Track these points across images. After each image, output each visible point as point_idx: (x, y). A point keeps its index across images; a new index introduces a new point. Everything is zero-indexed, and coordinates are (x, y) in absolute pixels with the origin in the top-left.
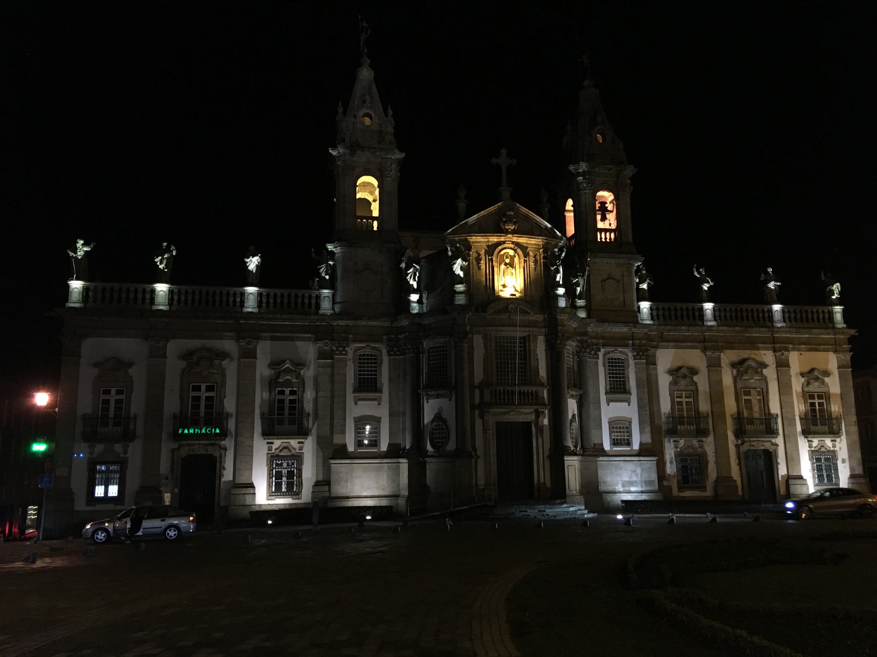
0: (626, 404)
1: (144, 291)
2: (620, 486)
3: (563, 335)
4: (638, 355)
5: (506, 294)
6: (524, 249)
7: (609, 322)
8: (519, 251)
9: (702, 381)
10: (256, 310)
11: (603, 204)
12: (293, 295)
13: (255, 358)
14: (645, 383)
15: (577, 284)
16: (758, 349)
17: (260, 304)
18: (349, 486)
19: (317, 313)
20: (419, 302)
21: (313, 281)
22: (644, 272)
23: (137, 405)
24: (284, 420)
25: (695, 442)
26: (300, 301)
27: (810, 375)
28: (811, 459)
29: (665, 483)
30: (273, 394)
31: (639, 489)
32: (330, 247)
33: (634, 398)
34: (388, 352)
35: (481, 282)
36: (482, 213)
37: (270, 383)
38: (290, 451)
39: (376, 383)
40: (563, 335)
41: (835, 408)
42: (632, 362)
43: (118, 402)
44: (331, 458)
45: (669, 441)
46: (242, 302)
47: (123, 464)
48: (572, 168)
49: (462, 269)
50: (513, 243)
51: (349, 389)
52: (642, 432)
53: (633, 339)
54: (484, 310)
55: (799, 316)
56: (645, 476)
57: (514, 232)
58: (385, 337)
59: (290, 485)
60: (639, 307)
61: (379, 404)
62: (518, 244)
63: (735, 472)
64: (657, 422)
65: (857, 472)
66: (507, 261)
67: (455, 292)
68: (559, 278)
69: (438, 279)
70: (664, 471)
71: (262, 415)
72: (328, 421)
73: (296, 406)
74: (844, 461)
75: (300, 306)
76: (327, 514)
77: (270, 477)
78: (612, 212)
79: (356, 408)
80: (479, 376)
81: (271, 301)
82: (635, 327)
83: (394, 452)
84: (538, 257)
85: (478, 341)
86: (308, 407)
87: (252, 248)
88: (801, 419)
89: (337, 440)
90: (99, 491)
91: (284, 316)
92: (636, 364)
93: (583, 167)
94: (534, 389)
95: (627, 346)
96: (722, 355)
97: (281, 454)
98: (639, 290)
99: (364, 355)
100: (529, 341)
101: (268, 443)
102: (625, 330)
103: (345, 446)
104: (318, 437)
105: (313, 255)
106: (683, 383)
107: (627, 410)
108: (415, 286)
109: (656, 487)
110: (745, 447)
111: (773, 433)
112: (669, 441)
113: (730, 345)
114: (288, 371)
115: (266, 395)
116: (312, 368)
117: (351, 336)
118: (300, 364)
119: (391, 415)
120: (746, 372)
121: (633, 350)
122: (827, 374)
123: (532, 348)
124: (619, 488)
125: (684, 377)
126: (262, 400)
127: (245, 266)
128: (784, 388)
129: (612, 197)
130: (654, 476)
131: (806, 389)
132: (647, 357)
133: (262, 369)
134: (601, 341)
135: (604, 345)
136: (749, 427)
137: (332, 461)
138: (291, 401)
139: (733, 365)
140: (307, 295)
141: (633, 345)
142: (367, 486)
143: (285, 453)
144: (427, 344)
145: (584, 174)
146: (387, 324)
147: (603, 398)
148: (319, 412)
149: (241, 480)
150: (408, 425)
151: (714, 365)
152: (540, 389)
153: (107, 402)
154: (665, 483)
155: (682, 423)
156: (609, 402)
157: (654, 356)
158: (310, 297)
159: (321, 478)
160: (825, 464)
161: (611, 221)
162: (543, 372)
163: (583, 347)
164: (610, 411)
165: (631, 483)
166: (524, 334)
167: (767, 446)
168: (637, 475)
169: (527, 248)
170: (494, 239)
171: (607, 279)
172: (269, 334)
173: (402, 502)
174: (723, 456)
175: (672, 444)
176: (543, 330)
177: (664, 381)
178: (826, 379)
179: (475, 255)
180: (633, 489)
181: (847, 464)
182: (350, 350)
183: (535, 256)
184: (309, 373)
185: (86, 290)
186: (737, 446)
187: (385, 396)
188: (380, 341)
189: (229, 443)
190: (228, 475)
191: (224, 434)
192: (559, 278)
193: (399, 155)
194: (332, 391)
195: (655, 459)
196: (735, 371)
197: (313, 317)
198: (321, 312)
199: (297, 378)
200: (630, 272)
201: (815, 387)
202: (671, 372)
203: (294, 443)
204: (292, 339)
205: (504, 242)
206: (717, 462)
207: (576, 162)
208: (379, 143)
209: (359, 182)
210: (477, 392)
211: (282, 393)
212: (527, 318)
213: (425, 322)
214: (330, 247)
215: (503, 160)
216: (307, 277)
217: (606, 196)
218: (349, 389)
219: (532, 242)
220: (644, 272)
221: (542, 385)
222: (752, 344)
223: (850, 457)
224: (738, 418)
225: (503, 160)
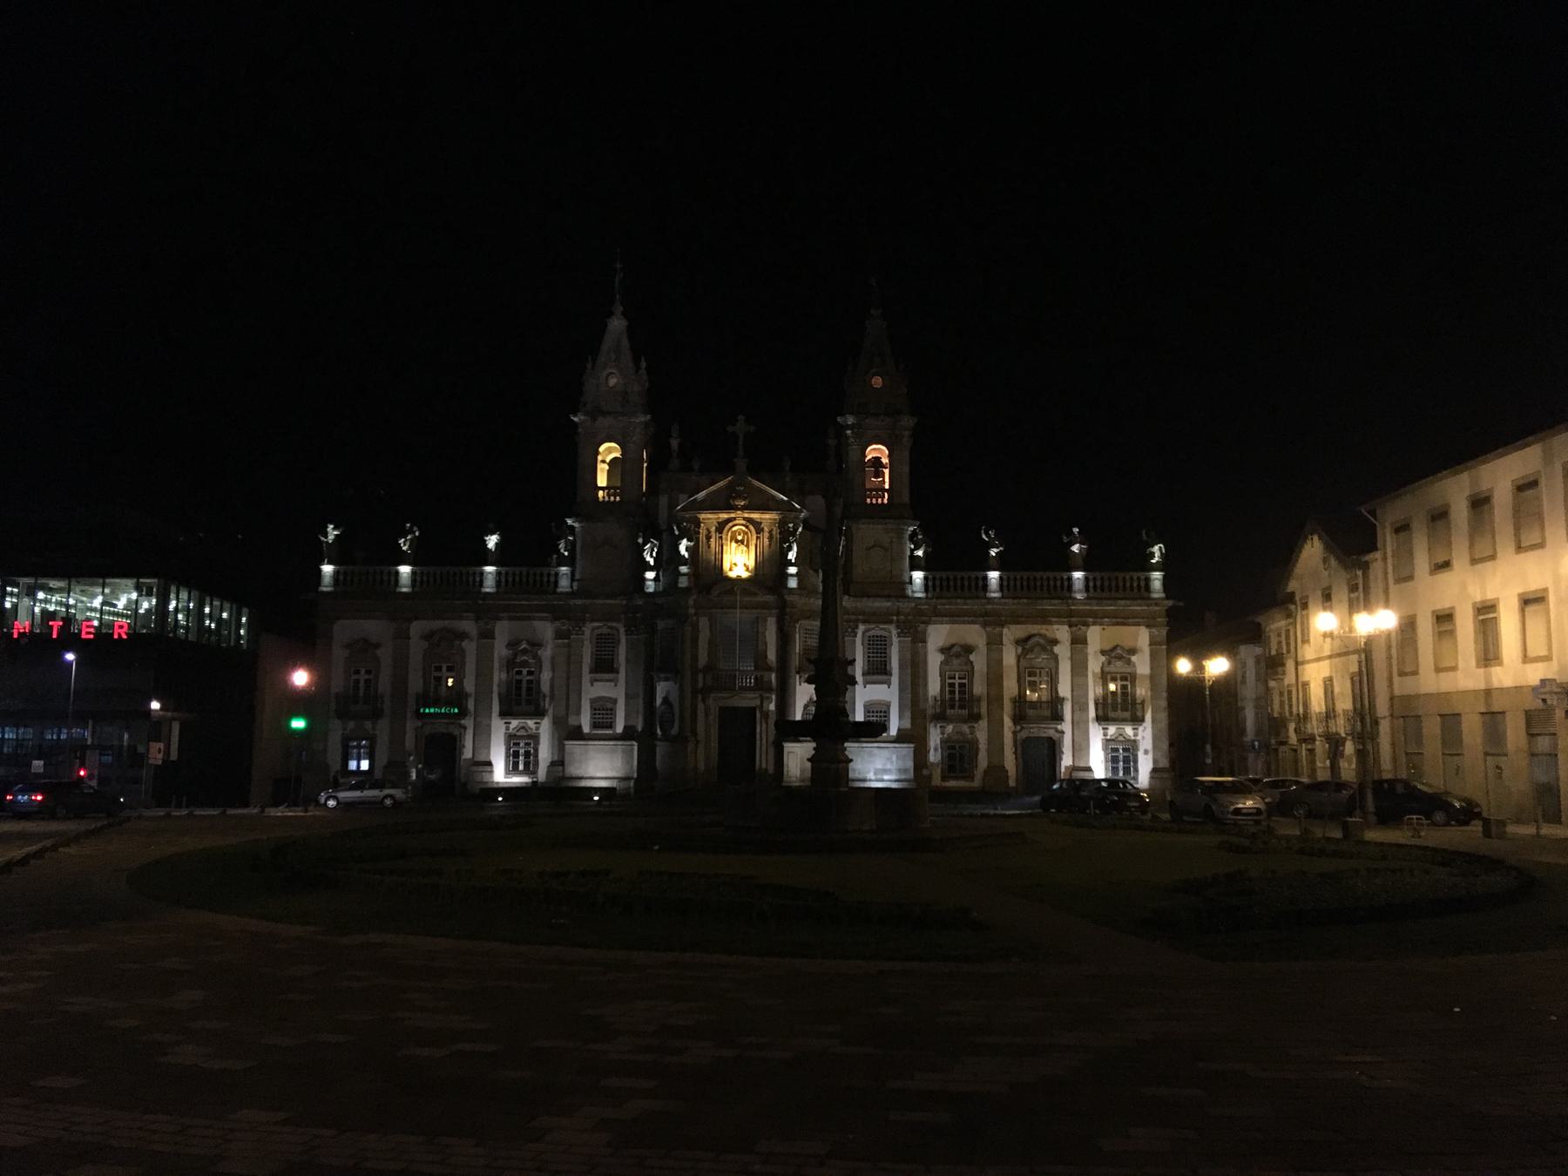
1: (389, 573)
5: (733, 575)
9: (979, 661)
11: (878, 459)
16: (1051, 623)
19: (555, 592)
20: (656, 579)
23: (384, 684)
24: (521, 700)
25: (965, 728)
27: (1117, 654)
28: (1105, 748)
29: (925, 772)
33: (895, 679)
41: (1142, 691)
42: (895, 640)
43: (366, 681)
46: (481, 582)
47: (372, 740)
48: (839, 419)
51: (586, 669)
52: (900, 717)
53: (898, 614)
55: (1106, 583)
57: (744, 508)
59: (527, 764)
62: (750, 520)
63: (1010, 761)
65: (1161, 765)
68: (792, 556)
69: (668, 560)
73: (533, 687)
74: (1146, 752)
76: (557, 794)
77: (507, 756)
79: (594, 689)
80: (703, 660)
83: (628, 734)
85: (704, 623)
88: (1096, 704)
89: (572, 721)
90: (353, 765)
95: (891, 622)
96: (1005, 631)
98: (912, 557)
103: (580, 727)
106: (956, 662)
107: (887, 693)
109: (911, 775)
110: (1024, 734)
111: (1059, 718)
113: (1016, 619)
114: (525, 651)
115: (504, 676)
118: (536, 644)
119: (627, 695)
120: (1031, 650)
122: (1133, 651)
124: (871, 776)
125: (958, 656)
127: (484, 543)
128: (1079, 668)
130: (910, 764)
131: (1107, 669)
133: (500, 650)
135: (864, 622)
136: (1031, 712)
138: (530, 682)
139: (1018, 642)
142: (601, 767)
143: (523, 733)
144: (661, 625)
145: (851, 427)
149: (482, 758)
150: (641, 709)
151: (995, 643)
153: (357, 681)
154: (925, 772)
155: (952, 707)
156: (866, 683)
157: (924, 632)
160: (1122, 755)
162: (772, 655)
165: (885, 771)
167: (1051, 733)
173: (632, 784)
174: (998, 742)
177: (934, 661)
178: (1134, 658)
181: (1150, 756)
182: (587, 629)
184: (546, 653)
185: (336, 574)
186: (1015, 733)
189: (468, 722)
190: (468, 753)
191: (463, 713)
192: (792, 556)
193: (643, 418)
196: (1020, 650)
201: (1119, 667)
202: (942, 650)
203: (531, 723)
204: (529, 618)
206: (988, 751)
207: (843, 415)
209: (602, 449)
211: (519, 673)
213: (659, 601)
214: (569, 522)
215: (740, 427)
216: (544, 553)
217: (877, 451)
218: (586, 669)
219: (767, 518)
221: (770, 669)
222: (1044, 618)
223: (1155, 747)
224: (1020, 701)
225: (740, 427)
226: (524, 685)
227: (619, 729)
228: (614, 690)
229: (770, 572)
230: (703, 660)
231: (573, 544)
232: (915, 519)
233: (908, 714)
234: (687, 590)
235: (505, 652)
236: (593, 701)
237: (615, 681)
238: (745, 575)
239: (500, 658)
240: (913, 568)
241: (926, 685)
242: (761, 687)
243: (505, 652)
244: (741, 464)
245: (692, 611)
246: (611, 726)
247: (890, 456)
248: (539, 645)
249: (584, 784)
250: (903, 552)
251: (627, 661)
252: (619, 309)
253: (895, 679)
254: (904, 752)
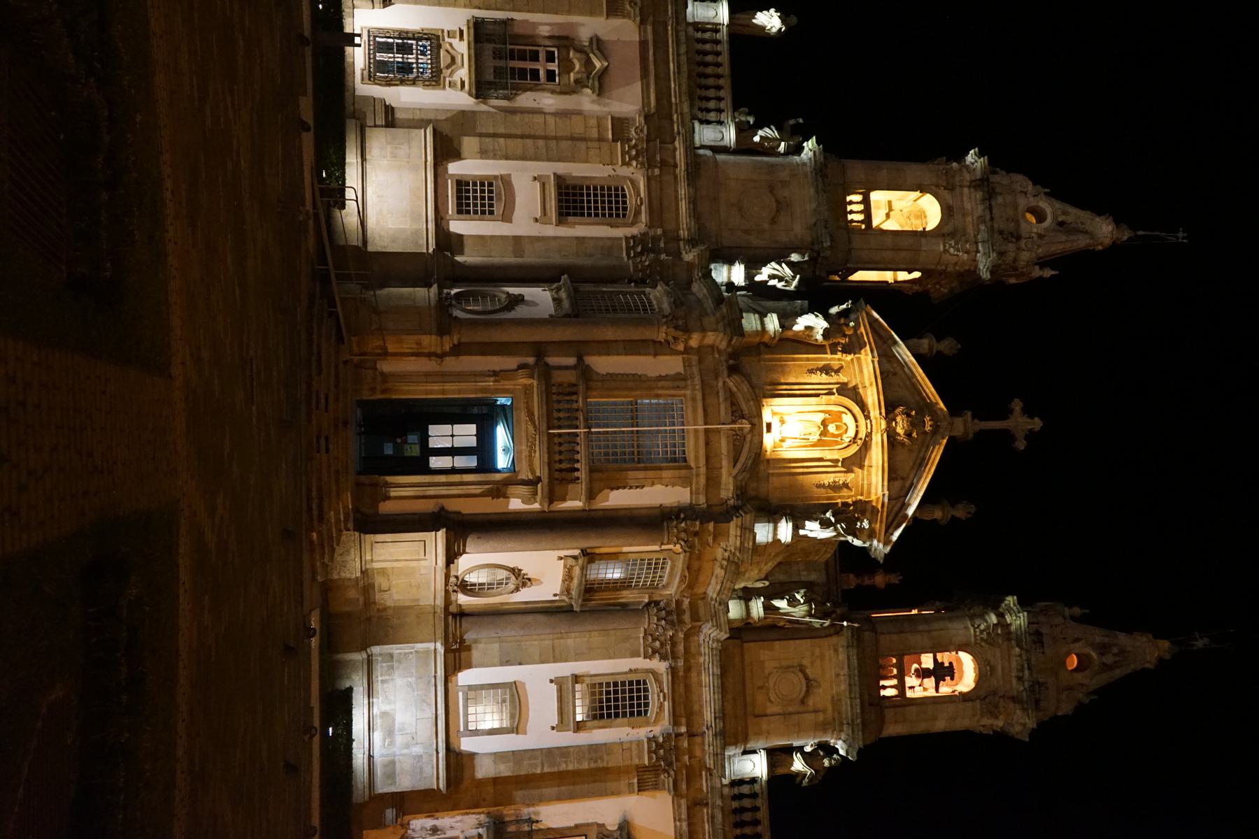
0: (555, 722)
2: (385, 708)
3: (696, 534)
4: (659, 746)
6: (856, 461)
7: (723, 674)
8: (854, 449)
10: (690, 19)
12: (721, 82)
13: (608, 16)
14: (600, 764)
15: (793, 602)
17: (699, 27)
18: (385, 162)
19: (694, 118)
20: (730, 286)
21: (749, 114)
22: (826, 763)
26: (712, 93)
29: (390, 813)
30: (547, 42)
31: (377, 752)
32: (810, 145)
34: (633, 237)
35: (783, 373)
36: (919, 372)
37: (567, 38)
38: (448, 67)
39: (575, 215)
40: (696, 534)
42: (642, 733)
44: (435, 130)
45: (480, 825)
48: (1011, 600)
49: (809, 328)
50: (869, 435)
51: (563, 168)
52: (499, 757)
53: (691, 735)
54: (733, 370)
56: (404, 765)
58: (659, 231)
60: (754, 752)
61: (536, 220)
62: (866, 446)
64: (519, 794)
66: (832, 428)
67: (763, 315)
68: (813, 529)
70: (418, 812)
71: (507, 23)
72: (502, 130)
75: (704, 93)
77: (403, 34)
78: (937, 689)
79: (528, 182)
80: (602, 364)
81: (708, 47)
82: (715, 735)
83: (448, 242)
84: (845, 492)
85: (671, 364)
86: (526, 100)
87: (794, 20)
91: (684, 58)
92: (639, 743)
93: (1018, 620)
94: (583, 474)
95: (676, 723)
97: (442, 52)
98: (789, 751)
99: (624, 196)
100: (679, 468)
101: (461, 32)
102: (708, 715)
103: (457, 155)
104: (473, 112)
105: (792, 122)
108: (758, 278)
109: (382, 788)
112: (480, 825)
114: (588, 64)
115: (544, 31)
116: (596, 108)
117: (657, 171)
118: (601, 84)
119: (517, 240)
121: (667, 737)
123: (665, 474)
124: (379, 706)
126: (535, 25)
129: (965, 690)
130: (404, 783)
132: (654, 769)
134: (681, 663)
135: (673, 671)
137: (429, 131)
138: (535, 74)
140: (722, 105)
141: (678, 735)
142: (386, 195)
143: (444, 59)
145: (1002, 624)
146: (683, 233)
148: (518, 118)
152: (582, 487)
154: (390, 813)
156: (559, 682)
157: (656, 787)
158: (720, 111)
159: (399, 115)
161: (919, 689)
162: (617, 499)
163: (669, 613)
164: (538, 679)
165: (390, 733)
166: (691, 457)
168: (407, 746)
169: (861, 467)
170: (872, 396)
171: (807, 678)
172: (650, 37)
175: (474, 832)
176: (702, 499)
179: (835, 364)
180: (377, 736)
183: (845, 485)
184: (586, 101)
187: (551, 230)
188: (651, 225)
192: (813, 529)
194: (556, 138)
195: (442, 785)
197: (686, 109)
198: (697, 124)
199: (576, 81)
200: (824, 727)
203: (463, 73)
205: (867, 417)
207: (1023, 603)
208: (1001, 232)
210: (571, 361)
211: (550, 58)
212: (725, 463)
213: (698, 288)
215: (1021, 423)
218: (563, 168)
219: (873, 482)
220: (826, 763)
221: (591, 496)
226: (530, 65)
227: (457, 226)
228: (527, 218)
229: (770, 489)
230: (602, 364)
231: (772, 152)
232: (860, 752)
233: (505, 770)
234: (739, 331)
235: (584, 35)
236: (506, 181)
237: (541, 220)
238: (769, 441)
239: (572, 26)
240: (771, 753)
241: (560, 798)
242: (560, 476)
243: (584, 35)
244: (965, 425)
245: (694, 342)
246: (462, 210)
247: (964, 697)
248: (601, 91)
249: (352, 158)
250: (800, 730)
252: (1126, 235)
254: (429, 771)
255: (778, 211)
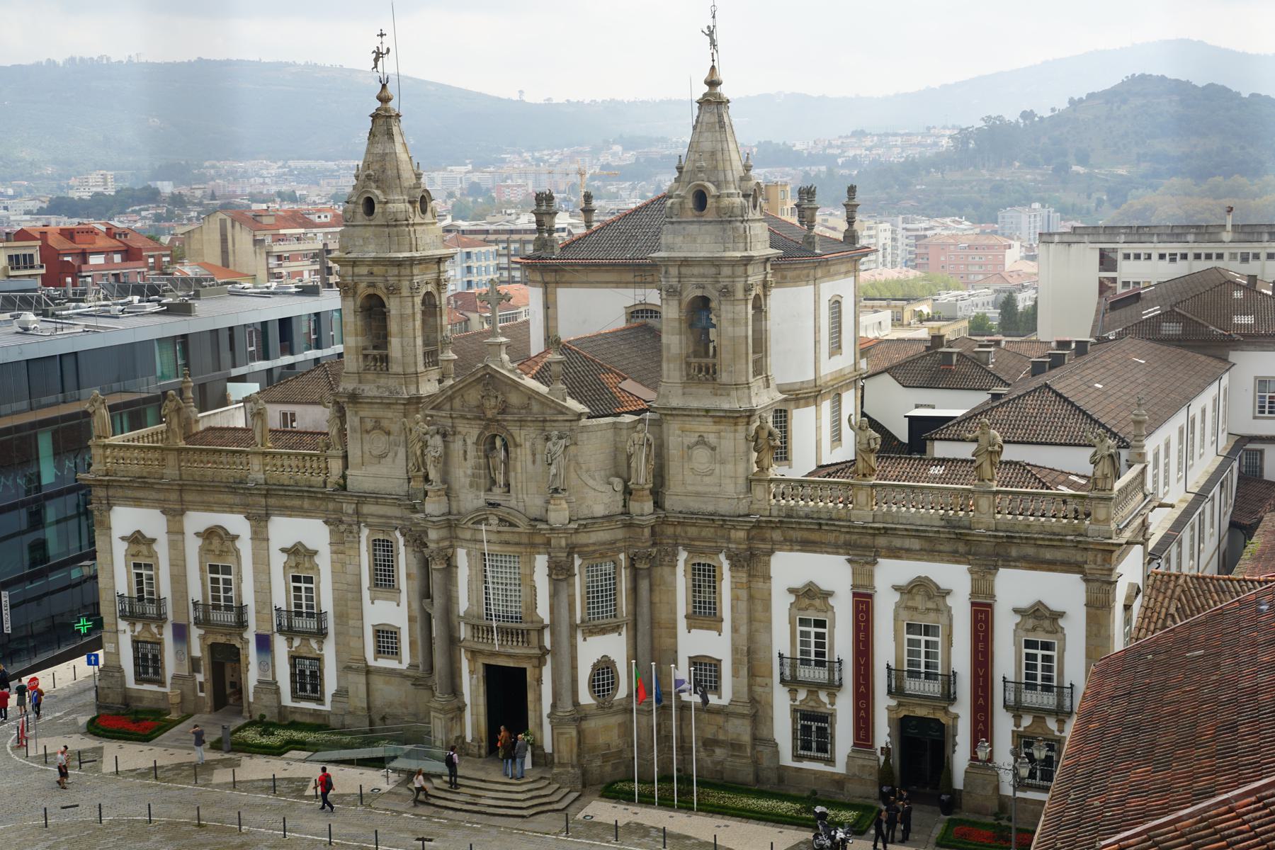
0: (716, 633)
147: (682, 623)
167: (940, 715)
177: (781, 605)
230: (463, 605)
251: (408, 576)
253: (727, 626)
255: (381, 428)
